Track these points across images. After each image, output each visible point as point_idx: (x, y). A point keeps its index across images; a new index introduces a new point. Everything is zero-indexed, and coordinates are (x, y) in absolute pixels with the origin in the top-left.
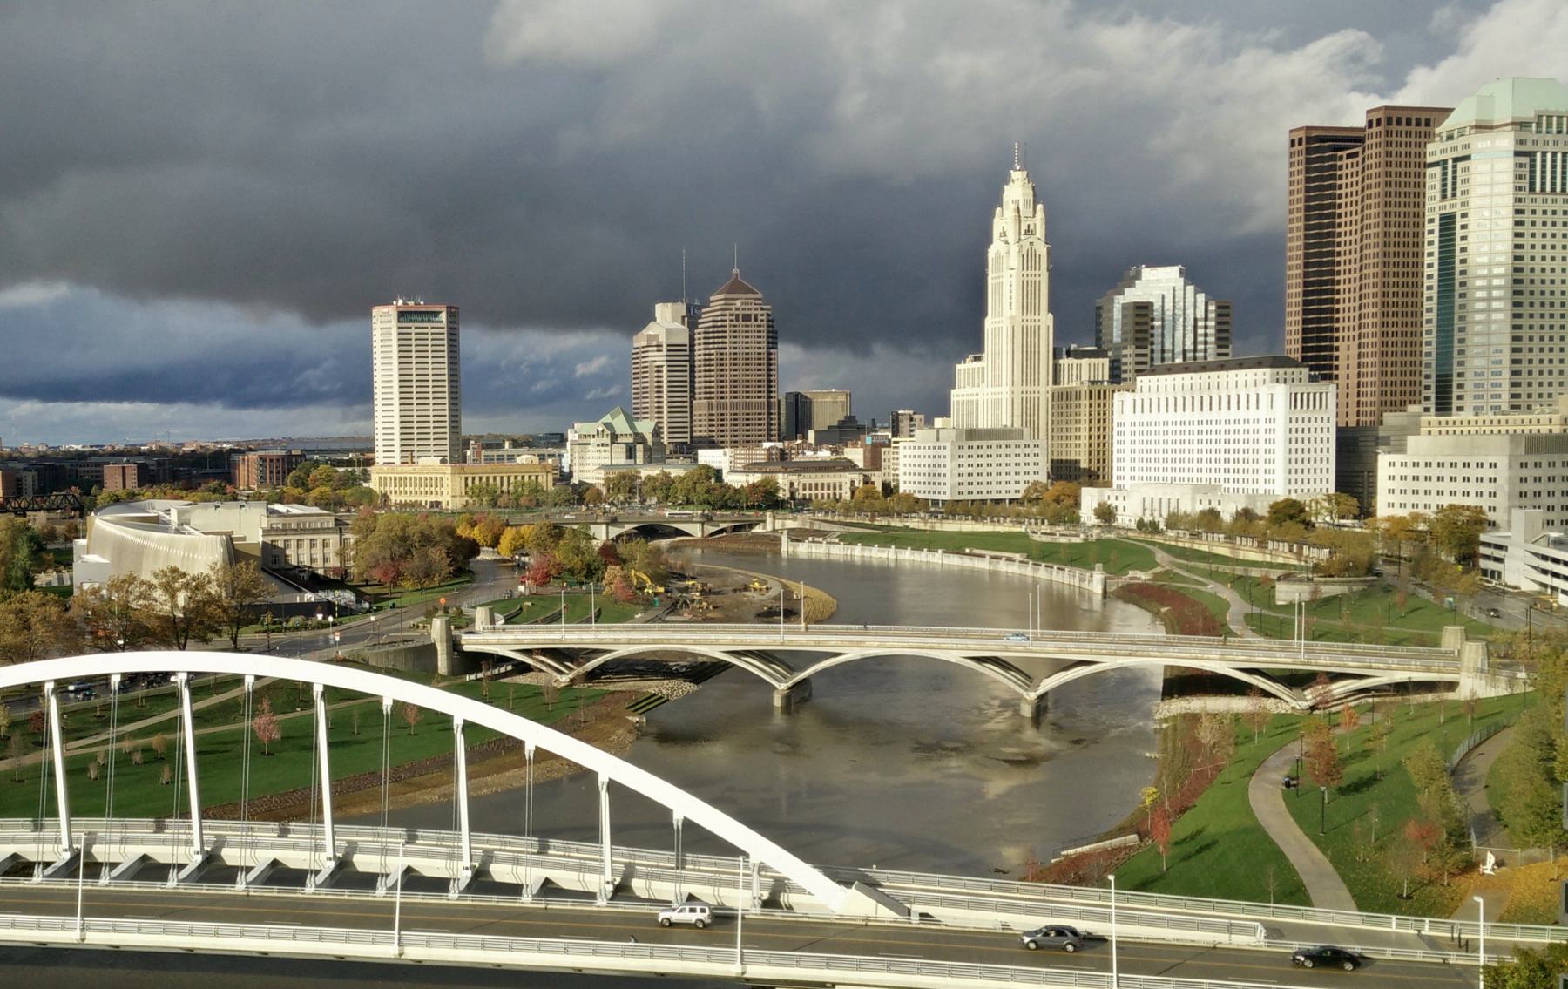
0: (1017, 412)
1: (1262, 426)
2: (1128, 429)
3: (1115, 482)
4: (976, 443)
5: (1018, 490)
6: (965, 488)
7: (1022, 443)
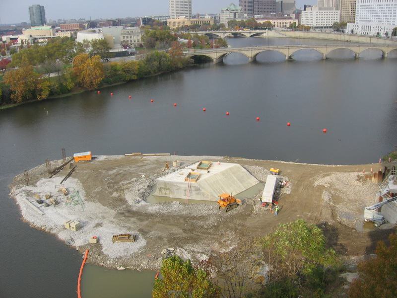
0: (334, 4)
1: (393, 6)
2: (360, 7)
3: (356, 22)
4: (321, 11)
5: (331, 24)
6: (318, 23)
7: (333, 11)
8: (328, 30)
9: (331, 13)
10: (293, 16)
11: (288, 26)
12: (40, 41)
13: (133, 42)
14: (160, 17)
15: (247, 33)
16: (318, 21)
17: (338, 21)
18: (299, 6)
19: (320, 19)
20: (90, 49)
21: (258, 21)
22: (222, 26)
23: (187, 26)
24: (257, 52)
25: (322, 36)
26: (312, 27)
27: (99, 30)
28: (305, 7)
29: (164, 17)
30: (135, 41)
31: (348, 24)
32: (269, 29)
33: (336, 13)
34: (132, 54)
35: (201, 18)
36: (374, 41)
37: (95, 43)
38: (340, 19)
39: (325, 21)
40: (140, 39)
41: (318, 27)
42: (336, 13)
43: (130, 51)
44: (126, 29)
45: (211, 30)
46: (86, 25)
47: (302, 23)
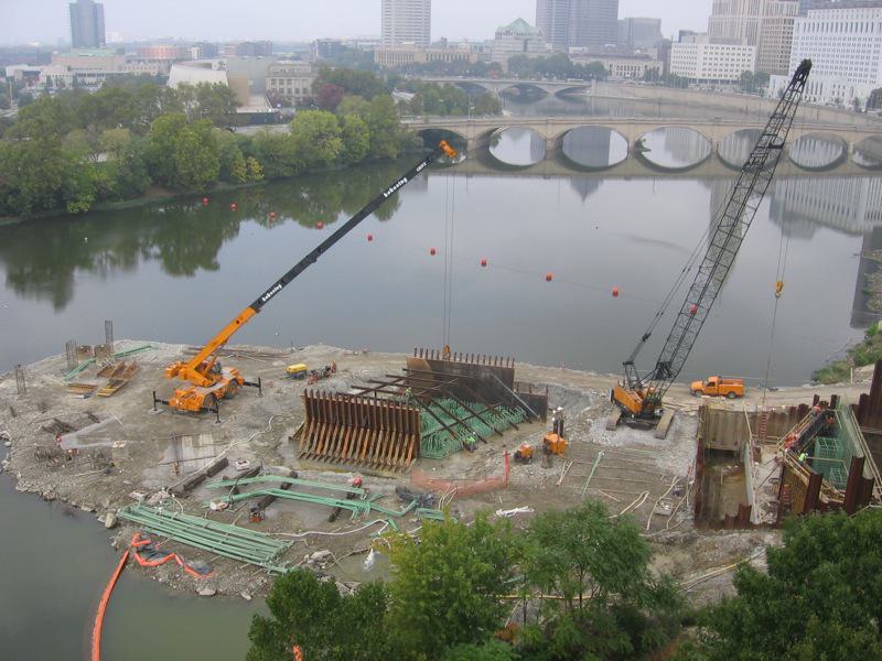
0: (744, 30)
1: (873, 43)
4: (715, 46)
5: (735, 75)
6: (707, 72)
8: (728, 89)
9: (736, 52)
10: (654, 53)
11: (642, 75)
12: (88, 80)
13: (293, 90)
14: (361, 41)
15: (551, 86)
16: (707, 67)
17: (752, 69)
18: (669, 32)
19: (713, 62)
20: (194, 104)
21: (575, 61)
22: (496, 66)
23: (417, 64)
24: (565, 128)
25: (713, 100)
26: (694, 80)
27: (221, 63)
28: (682, 33)
29: (368, 41)
30: (297, 91)
31: (772, 77)
32: (598, 80)
33: (747, 52)
34: (288, 119)
35: (451, 47)
36: (826, 116)
37: (205, 92)
38: (757, 65)
39: (724, 68)
40: (310, 89)
41: (706, 81)
42: (747, 52)
43: (284, 111)
44: (280, 65)
45: (470, 75)
46: (195, 52)
47: (672, 70)
